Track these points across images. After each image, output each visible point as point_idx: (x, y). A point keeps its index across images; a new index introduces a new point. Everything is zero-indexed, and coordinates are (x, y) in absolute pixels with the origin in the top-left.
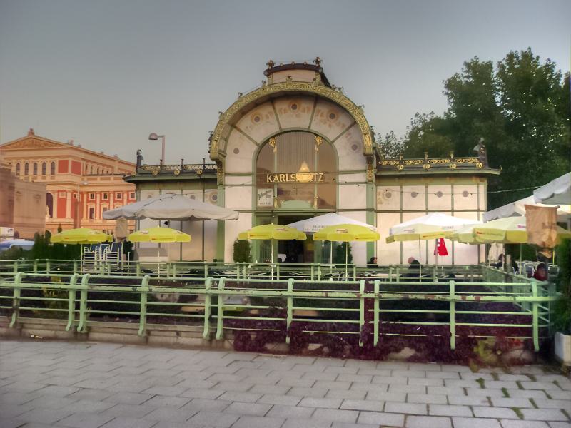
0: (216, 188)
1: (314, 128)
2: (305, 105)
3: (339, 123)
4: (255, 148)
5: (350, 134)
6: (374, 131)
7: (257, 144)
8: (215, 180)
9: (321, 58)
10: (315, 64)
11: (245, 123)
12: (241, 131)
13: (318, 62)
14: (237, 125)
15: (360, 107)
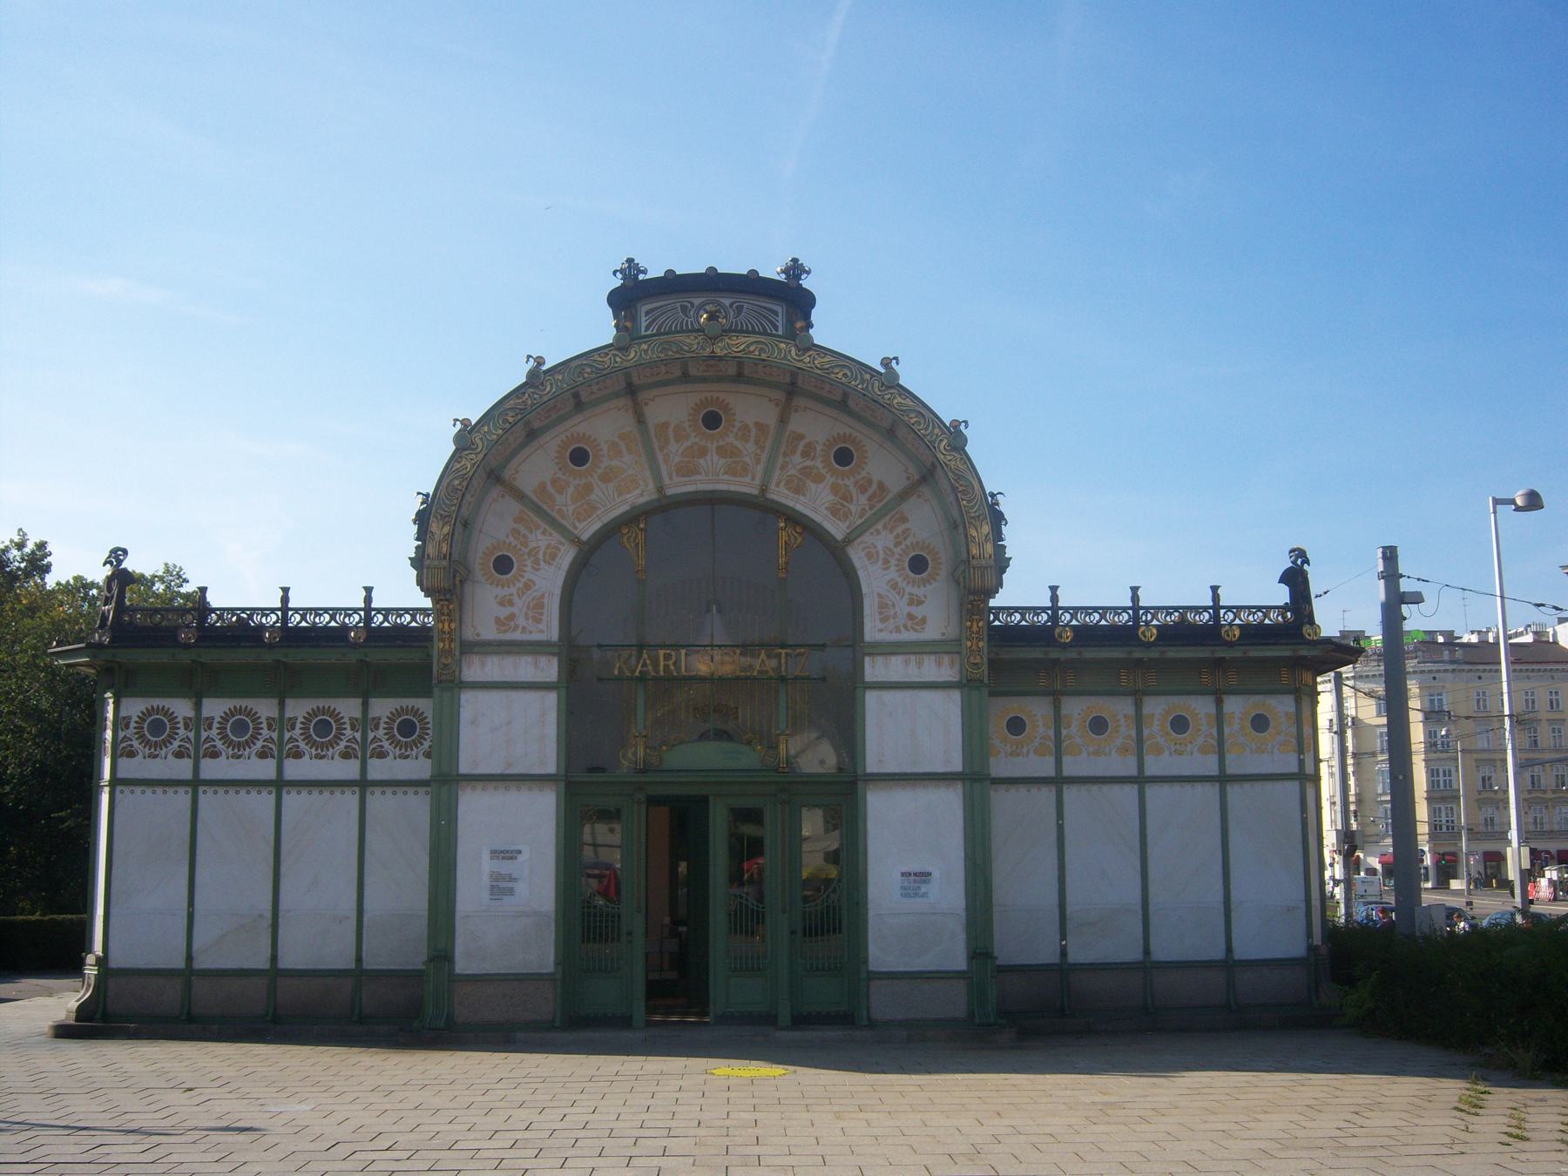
0: (427, 693)
1: (781, 494)
2: (751, 409)
3: (870, 482)
4: (567, 556)
5: (904, 520)
6: (1002, 508)
7: (575, 540)
8: (426, 668)
9: (805, 261)
10: (782, 277)
11: (537, 468)
12: (520, 496)
13: (795, 270)
14: (507, 474)
15: (956, 424)
